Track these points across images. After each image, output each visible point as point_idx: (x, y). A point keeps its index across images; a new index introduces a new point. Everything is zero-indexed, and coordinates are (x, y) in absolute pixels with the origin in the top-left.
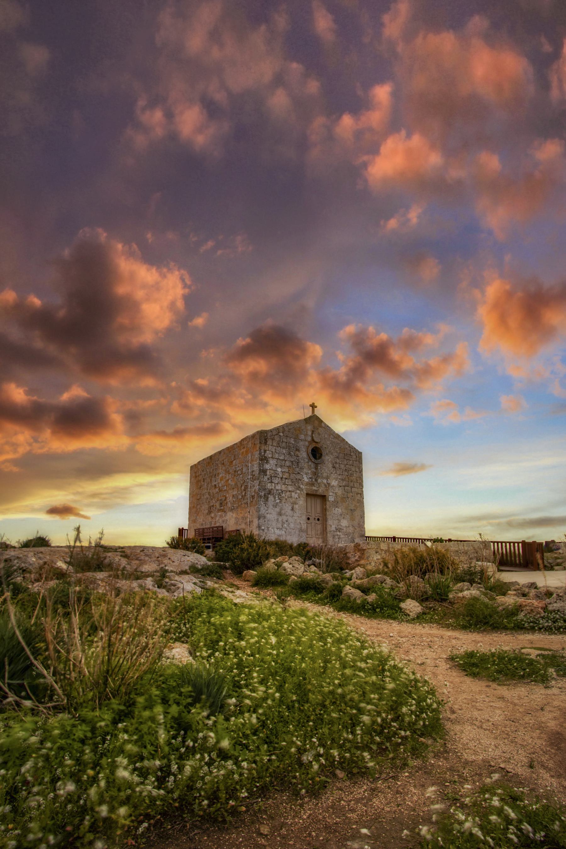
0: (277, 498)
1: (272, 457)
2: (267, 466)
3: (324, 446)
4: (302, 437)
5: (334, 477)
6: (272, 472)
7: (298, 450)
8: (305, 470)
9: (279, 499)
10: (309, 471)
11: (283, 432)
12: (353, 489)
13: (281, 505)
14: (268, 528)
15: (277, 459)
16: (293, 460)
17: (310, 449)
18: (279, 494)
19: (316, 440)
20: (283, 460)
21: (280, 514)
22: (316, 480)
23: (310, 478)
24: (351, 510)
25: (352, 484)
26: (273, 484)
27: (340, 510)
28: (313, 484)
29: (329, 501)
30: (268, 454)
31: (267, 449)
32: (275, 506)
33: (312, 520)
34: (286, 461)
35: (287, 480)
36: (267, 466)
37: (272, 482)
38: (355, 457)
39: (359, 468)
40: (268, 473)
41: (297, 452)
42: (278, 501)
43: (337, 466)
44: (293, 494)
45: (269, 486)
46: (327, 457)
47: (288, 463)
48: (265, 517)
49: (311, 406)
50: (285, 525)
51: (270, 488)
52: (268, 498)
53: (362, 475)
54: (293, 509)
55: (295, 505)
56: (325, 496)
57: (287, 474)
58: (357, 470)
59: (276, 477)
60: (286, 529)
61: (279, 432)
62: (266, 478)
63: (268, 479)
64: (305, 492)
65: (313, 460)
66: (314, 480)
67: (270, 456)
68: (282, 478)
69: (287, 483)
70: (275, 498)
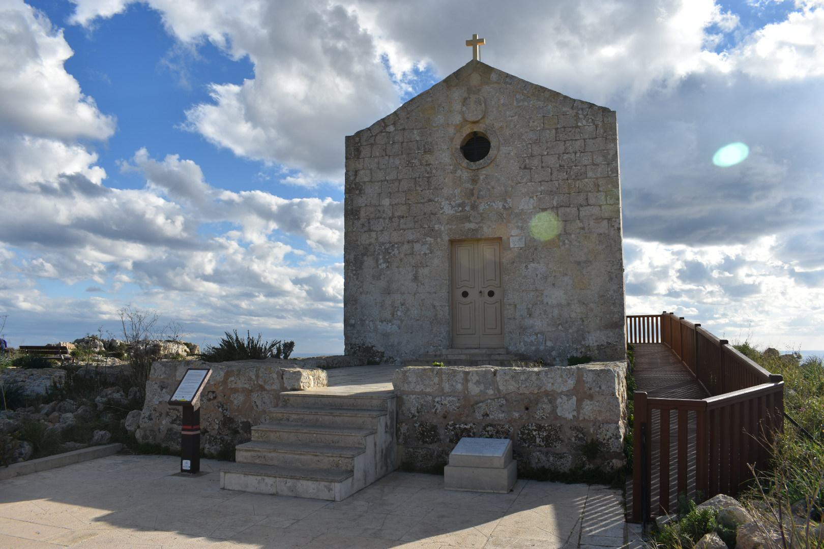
0: (382, 261)
1: (371, 181)
2: (361, 201)
3: (497, 125)
4: (440, 119)
5: (524, 190)
6: (372, 209)
7: (429, 151)
8: (446, 191)
9: (386, 261)
10: (457, 191)
11: (394, 124)
12: (584, 212)
13: (389, 272)
14: (363, 321)
15: (382, 181)
16: (417, 175)
17: (458, 142)
18: (387, 252)
19: (471, 118)
20: (393, 181)
21: (388, 291)
22: (474, 207)
23: (459, 205)
24: (578, 263)
25: (581, 198)
26: (373, 234)
27: (541, 268)
28: (467, 219)
29: (510, 249)
30: (364, 176)
31: (361, 167)
32: (377, 277)
33: (473, 294)
34: (400, 181)
35: (402, 221)
36: (361, 201)
37: (370, 230)
38: (592, 127)
39: (605, 156)
40: (363, 214)
41: (428, 157)
42: (384, 266)
43: (536, 162)
44: (417, 247)
45: (365, 239)
46: (504, 149)
47: (405, 185)
48: (356, 301)
49: (469, 43)
50: (399, 313)
51: (367, 242)
52: (362, 263)
53: (615, 170)
54: (416, 278)
55: (421, 271)
56: (501, 238)
57: (404, 208)
58: (599, 160)
59: (378, 218)
60: (402, 321)
61: (386, 126)
62: (358, 224)
63: (363, 225)
64: (446, 238)
65: (465, 162)
66: (467, 208)
67: (366, 179)
68: (391, 219)
69: (402, 226)
70: (377, 260)
